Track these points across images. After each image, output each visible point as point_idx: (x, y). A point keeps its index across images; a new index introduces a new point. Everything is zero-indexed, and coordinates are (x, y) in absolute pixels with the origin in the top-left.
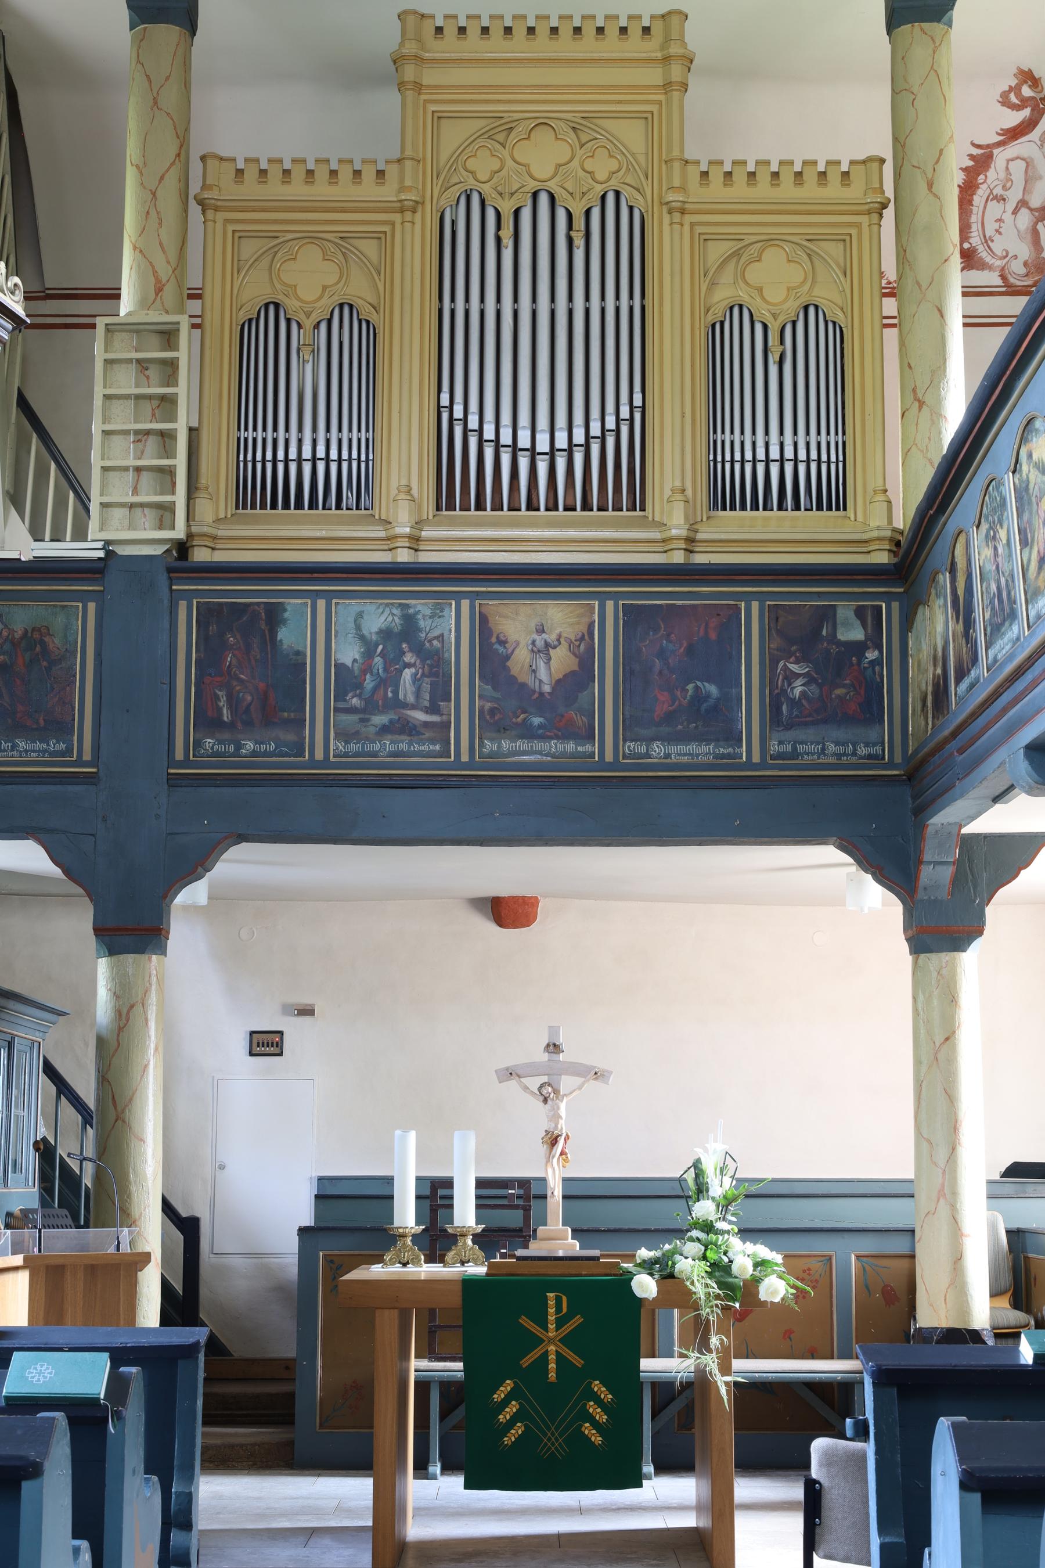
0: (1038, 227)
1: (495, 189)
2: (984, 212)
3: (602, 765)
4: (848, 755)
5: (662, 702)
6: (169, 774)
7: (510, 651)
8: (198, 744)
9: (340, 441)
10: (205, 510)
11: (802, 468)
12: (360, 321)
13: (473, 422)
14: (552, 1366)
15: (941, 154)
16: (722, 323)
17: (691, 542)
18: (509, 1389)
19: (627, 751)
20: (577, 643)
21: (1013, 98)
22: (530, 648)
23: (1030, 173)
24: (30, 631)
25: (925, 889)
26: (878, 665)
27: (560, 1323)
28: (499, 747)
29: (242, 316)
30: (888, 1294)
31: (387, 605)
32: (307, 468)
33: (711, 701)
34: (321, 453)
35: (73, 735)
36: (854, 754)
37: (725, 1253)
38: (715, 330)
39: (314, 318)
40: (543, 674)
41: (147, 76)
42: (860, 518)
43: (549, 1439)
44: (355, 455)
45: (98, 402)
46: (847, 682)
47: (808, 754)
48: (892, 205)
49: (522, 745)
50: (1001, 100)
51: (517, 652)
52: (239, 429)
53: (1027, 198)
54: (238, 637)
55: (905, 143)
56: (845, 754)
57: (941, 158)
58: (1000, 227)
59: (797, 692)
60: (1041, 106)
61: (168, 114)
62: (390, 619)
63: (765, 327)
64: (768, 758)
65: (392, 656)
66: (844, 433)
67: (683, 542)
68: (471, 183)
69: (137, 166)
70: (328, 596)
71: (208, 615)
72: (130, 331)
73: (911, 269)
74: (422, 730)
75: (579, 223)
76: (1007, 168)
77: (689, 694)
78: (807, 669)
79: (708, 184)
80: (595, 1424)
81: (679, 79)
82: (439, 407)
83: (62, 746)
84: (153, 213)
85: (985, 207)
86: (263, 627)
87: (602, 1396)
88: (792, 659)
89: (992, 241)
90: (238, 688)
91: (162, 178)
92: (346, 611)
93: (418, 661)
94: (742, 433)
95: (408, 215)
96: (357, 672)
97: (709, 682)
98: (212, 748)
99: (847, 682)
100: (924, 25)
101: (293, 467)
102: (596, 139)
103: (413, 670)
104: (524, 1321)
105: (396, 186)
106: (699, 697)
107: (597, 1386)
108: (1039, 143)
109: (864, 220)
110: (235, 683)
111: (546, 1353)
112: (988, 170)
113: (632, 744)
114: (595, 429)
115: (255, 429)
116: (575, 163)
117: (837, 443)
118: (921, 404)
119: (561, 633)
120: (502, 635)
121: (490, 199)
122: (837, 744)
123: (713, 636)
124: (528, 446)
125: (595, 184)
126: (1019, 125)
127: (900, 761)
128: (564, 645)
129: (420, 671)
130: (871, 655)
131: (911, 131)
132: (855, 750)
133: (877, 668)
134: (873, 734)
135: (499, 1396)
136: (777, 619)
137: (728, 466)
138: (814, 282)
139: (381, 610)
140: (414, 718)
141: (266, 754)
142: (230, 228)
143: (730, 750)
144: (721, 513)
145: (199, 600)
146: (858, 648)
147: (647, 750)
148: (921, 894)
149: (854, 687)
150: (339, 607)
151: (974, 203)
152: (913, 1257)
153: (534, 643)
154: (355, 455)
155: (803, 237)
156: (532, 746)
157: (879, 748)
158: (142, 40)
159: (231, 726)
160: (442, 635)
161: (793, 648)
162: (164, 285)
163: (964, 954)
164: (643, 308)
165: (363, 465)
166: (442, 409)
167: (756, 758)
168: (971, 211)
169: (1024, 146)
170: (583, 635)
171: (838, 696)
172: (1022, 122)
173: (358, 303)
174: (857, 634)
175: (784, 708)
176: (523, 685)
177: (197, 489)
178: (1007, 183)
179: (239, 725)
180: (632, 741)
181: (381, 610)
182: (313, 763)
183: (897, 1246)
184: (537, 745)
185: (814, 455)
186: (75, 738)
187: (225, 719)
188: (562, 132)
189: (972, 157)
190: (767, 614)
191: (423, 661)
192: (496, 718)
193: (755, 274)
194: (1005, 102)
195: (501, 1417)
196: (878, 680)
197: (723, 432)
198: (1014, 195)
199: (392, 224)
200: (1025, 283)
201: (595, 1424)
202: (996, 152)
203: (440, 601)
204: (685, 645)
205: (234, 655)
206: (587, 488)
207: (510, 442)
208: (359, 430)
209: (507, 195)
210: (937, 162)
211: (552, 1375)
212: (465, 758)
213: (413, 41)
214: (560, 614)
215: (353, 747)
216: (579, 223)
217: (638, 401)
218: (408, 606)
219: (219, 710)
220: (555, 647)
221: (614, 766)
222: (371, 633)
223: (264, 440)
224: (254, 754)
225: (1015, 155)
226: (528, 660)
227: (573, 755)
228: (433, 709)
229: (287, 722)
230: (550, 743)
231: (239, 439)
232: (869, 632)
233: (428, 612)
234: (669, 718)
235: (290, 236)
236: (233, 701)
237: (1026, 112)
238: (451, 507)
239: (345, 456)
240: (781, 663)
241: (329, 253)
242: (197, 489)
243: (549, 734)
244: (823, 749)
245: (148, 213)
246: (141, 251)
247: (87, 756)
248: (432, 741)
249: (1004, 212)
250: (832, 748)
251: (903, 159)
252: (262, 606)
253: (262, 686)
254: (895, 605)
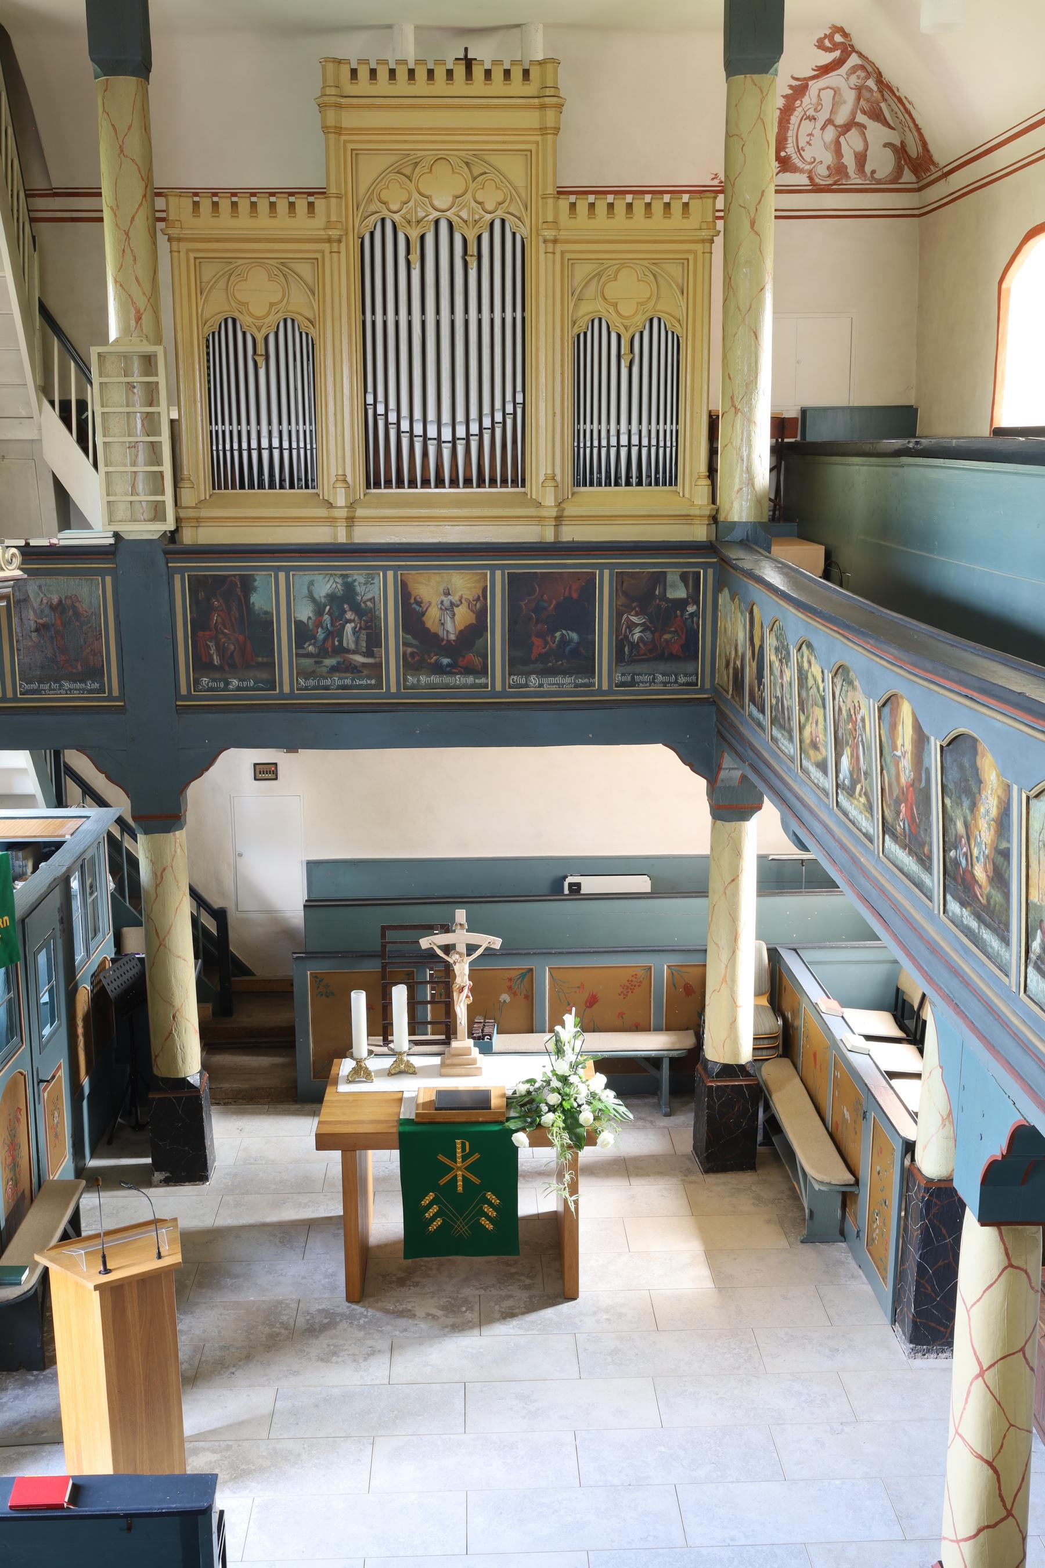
0: (840, 139)
1: (404, 218)
2: (798, 129)
3: (494, 694)
4: (672, 683)
5: (538, 647)
6: (177, 706)
7: (424, 609)
8: (197, 682)
9: (290, 432)
10: (188, 497)
11: (644, 451)
12: (301, 334)
13: (392, 417)
14: (460, 1183)
15: (762, 195)
16: (585, 334)
17: (559, 519)
18: (431, 1198)
19: (511, 682)
20: (474, 603)
21: (827, 43)
22: (439, 606)
23: (837, 99)
24: (63, 599)
25: (723, 781)
26: (696, 616)
27: (464, 1158)
28: (419, 680)
29: (207, 331)
30: (688, 990)
31: (331, 575)
32: (265, 454)
33: (573, 645)
34: (276, 443)
35: (104, 677)
36: (676, 682)
37: (575, 1100)
38: (579, 342)
39: (264, 332)
40: (449, 626)
41: (113, 125)
42: (687, 495)
43: (459, 1226)
44: (302, 445)
46: (673, 629)
47: (642, 682)
48: (722, 234)
49: (435, 679)
50: (817, 44)
51: (430, 610)
52: (211, 424)
53: (832, 117)
54: (221, 601)
55: (734, 183)
56: (669, 682)
57: (763, 198)
58: (811, 140)
59: (636, 637)
60: (849, 49)
61: (133, 160)
62: (334, 586)
63: (619, 337)
64: (614, 686)
65: (337, 614)
66: (677, 423)
67: (553, 520)
68: (385, 213)
69: (112, 208)
70: (287, 570)
71: (198, 585)
73: (734, 294)
74: (361, 669)
75: (473, 249)
76: (819, 96)
77: (557, 639)
78: (644, 620)
79: (575, 218)
80: (488, 1218)
81: (553, 125)
82: (366, 404)
83: (96, 685)
84: (128, 251)
85: (799, 125)
86: (239, 593)
87: (493, 1201)
88: (633, 613)
89: (804, 150)
90: (223, 640)
91: (133, 219)
92: (301, 581)
93: (356, 618)
94: (600, 423)
95: (335, 245)
96: (311, 627)
97: (572, 631)
98: (208, 685)
99: (673, 629)
100: (755, 77)
101: (255, 454)
102: (486, 173)
103: (353, 625)
104: (441, 1157)
105: (324, 219)
106: (564, 642)
107: (489, 1195)
108: (845, 76)
109: (699, 247)
110: (221, 636)
111: (455, 1179)
112: (803, 97)
113: (515, 677)
114: (487, 422)
115: (223, 423)
116: (469, 195)
117: (672, 431)
118: (737, 411)
119: (462, 595)
120: (418, 597)
121: (400, 227)
122: (664, 675)
123: (575, 595)
124: (435, 436)
125: (484, 213)
126: (830, 63)
127: (709, 687)
128: (465, 603)
129: (358, 625)
130: (691, 609)
131: (740, 173)
132: (677, 679)
133: (695, 619)
134: (690, 668)
135: (425, 1202)
136: (623, 582)
137: (588, 450)
138: (658, 298)
139: (327, 579)
140: (355, 661)
141: (247, 689)
142: (192, 255)
143: (586, 680)
144: (582, 489)
145: (189, 573)
146: (682, 604)
147: (526, 681)
148: (719, 783)
149: (678, 634)
150: (296, 577)
151: (791, 122)
152: (705, 966)
153: (442, 603)
154: (302, 445)
155: (649, 261)
156: (442, 680)
157: (694, 678)
158: (105, 91)
159: (220, 668)
160: (374, 598)
161: (634, 605)
162: (142, 314)
163: (747, 822)
164: (523, 319)
165: (309, 452)
166: (368, 407)
167: (605, 687)
168: (788, 128)
169: (834, 79)
170: (479, 597)
171: (667, 641)
172: (834, 61)
173: (299, 319)
174: (680, 593)
175: (626, 649)
176: (436, 636)
177: (182, 479)
178: (818, 107)
179: (227, 668)
180: (515, 675)
181: (327, 579)
182: (282, 696)
183: (694, 960)
184: (447, 679)
185: (654, 442)
186: (106, 679)
187: (216, 663)
188: (457, 167)
189: (791, 87)
190: (615, 579)
191: (360, 618)
192: (416, 659)
193: (613, 290)
194: (820, 45)
195: (427, 1215)
196: (696, 627)
197: (585, 423)
198: (823, 116)
199: (323, 252)
200: (827, 183)
201: (488, 1218)
202: (810, 83)
203: (371, 572)
204: (554, 602)
205: (218, 615)
206: (481, 463)
207: (421, 433)
208: (304, 424)
209: (414, 223)
210: (759, 202)
211: (460, 1189)
212: (393, 690)
213: (332, 88)
214: (461, 581)
215: (312, 682)
216: (473, 249)
217: (519, 398)
218: (347, 576)
219: (211, 656)
220: (458, 606)
221: (503, 694)
222: (320, 597)
223: (231, 432)
224: (239, 689)
225: (825, 86)
226: (438, 616)
227: (473, 686)
228: (369, 654)
229: (260, 666)
230: (455, 678)
231: (211, 432)
232: (690, 591)
233: (363, 580)
234: (543, 658)
235: (240, 262)
236: (221, 650)
237: (837, 54)
238: (377, 485)
239: (294, 445)
240: (625, 616)
241: (273, 276)
242: (182, 479)
243: (454, 670)
244: (654, 679)
245: (124, 251)
246: (121, 285)
247: (116, 693)
248: (369, 677)
249: (814, 128)
250: (660, 678)
251: (732, 196)
252: (238, 577)
253: (241, 638)
254: (710, 571)
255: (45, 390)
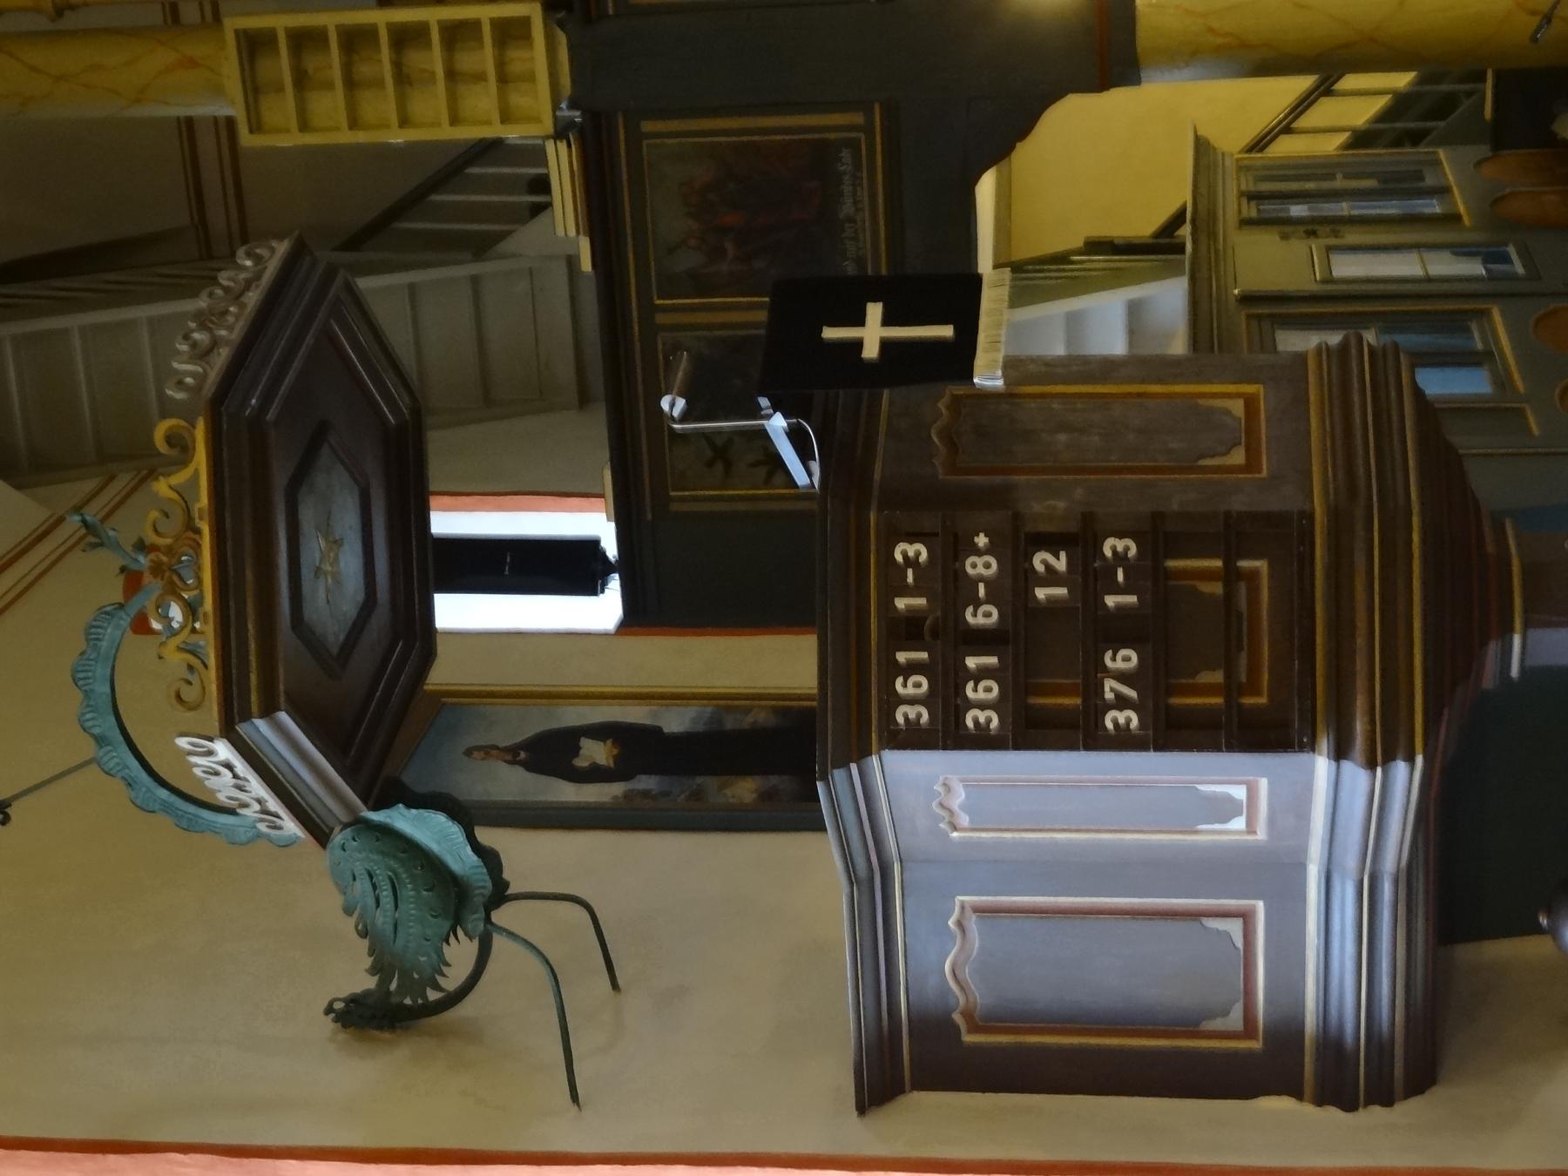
45: (361, 137)
72: (256, 101)
91: (33, 69)
247: (858, 118)
255: (482, 246)
